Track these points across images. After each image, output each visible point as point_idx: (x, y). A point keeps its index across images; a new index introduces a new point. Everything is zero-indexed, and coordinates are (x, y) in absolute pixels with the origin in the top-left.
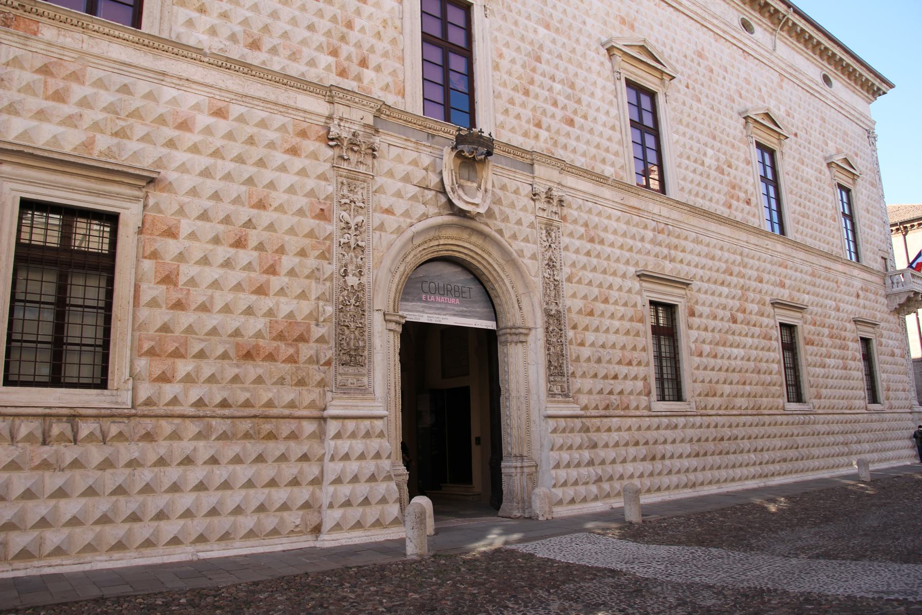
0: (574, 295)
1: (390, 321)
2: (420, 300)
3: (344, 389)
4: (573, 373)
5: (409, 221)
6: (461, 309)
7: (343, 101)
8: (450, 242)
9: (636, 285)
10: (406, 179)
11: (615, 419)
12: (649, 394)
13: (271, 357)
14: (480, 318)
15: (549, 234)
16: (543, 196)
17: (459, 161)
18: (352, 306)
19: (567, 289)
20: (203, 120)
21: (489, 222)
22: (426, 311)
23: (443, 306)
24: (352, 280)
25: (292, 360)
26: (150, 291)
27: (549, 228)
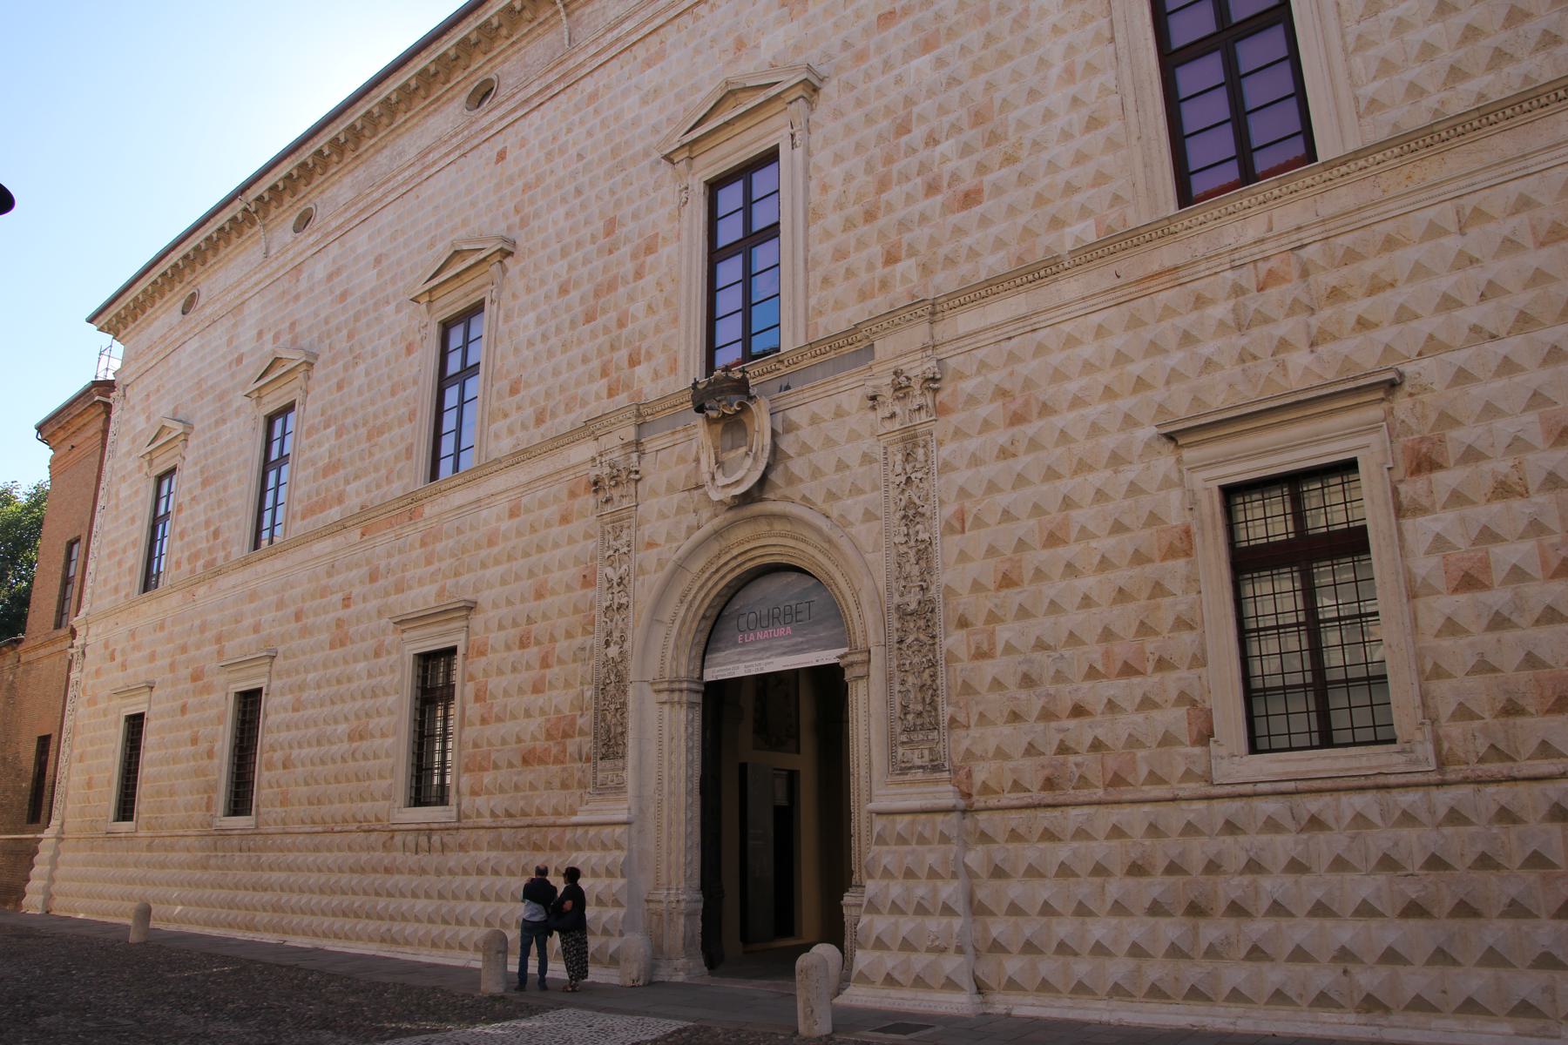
0: (963, 557)
1: (660, 691)
2: (736, 645)
3: (602, 789)
4: (953, 720)
5: (675, 545)
6: (794, 640)
7: (604, 430)
8: (748, 547)
9: (1165, 462)
10: (671, 489)
11: (1073, 812)
12: (1205, 736)
13: (541, 761)
14: (826, 648)
15: (908, 457)
16: (887, 393)
17: (719, 428)
18: (611, 685)
19: (946, 548)
20: (506, 525)
21: (788, 492)
22: (744, 658)
23: (766, 644)
24: (613, 651)
25: (557, 761)
26: (473, 710)
27: (910, 442)
